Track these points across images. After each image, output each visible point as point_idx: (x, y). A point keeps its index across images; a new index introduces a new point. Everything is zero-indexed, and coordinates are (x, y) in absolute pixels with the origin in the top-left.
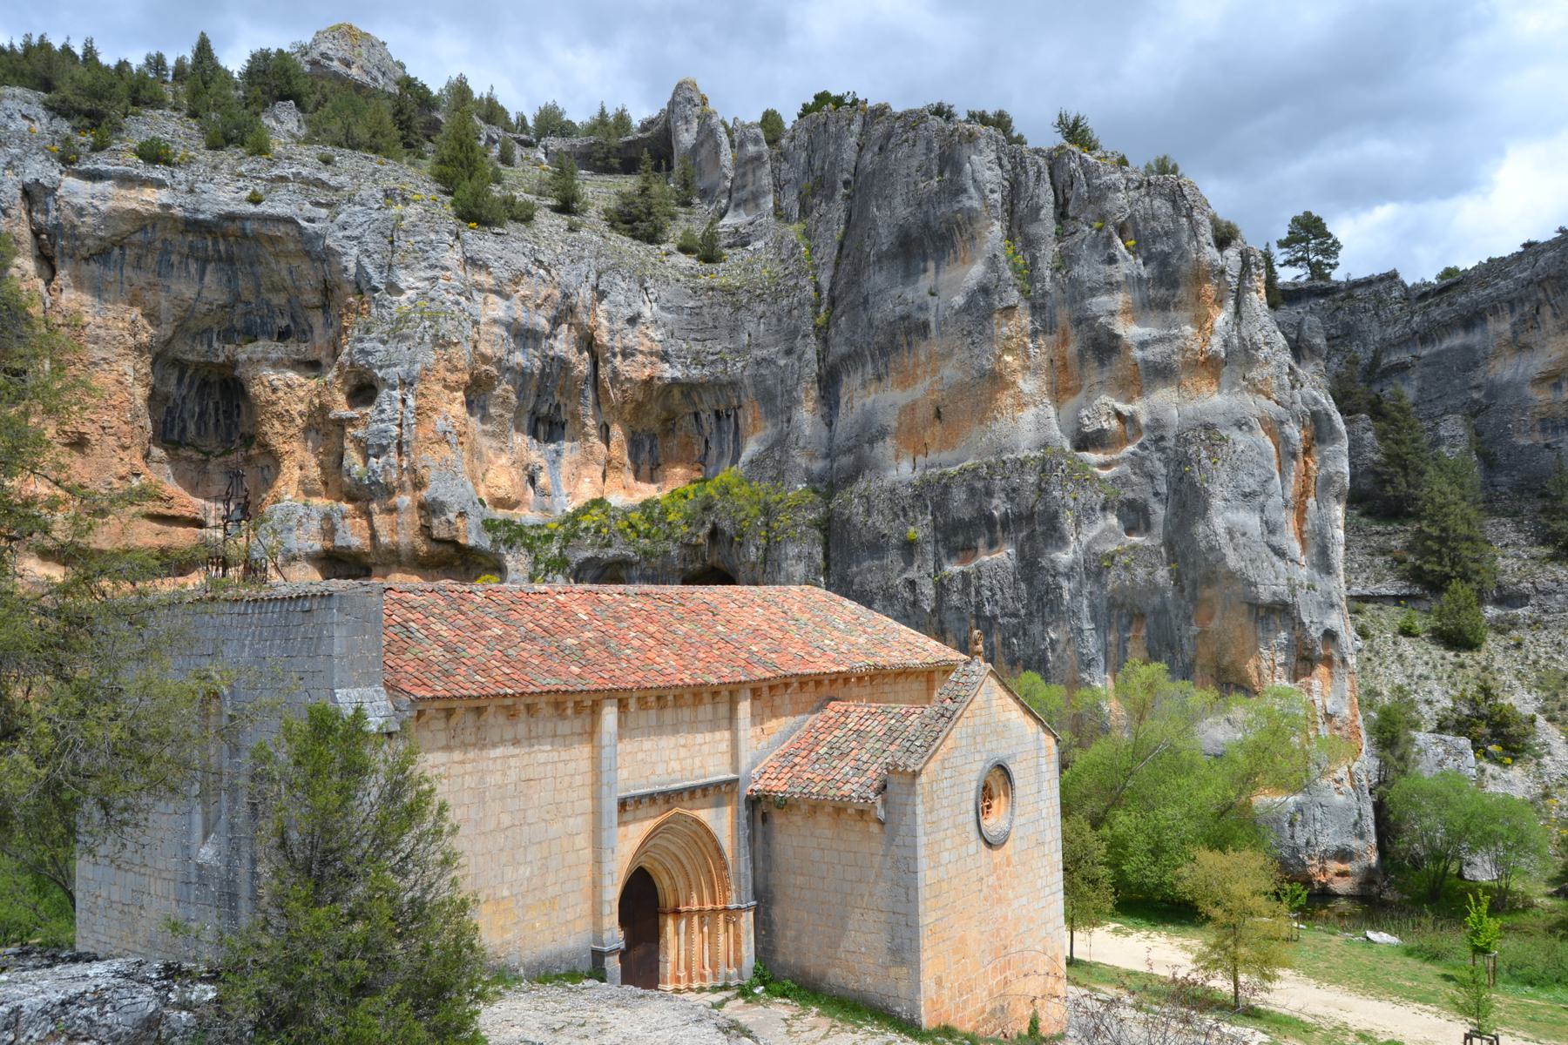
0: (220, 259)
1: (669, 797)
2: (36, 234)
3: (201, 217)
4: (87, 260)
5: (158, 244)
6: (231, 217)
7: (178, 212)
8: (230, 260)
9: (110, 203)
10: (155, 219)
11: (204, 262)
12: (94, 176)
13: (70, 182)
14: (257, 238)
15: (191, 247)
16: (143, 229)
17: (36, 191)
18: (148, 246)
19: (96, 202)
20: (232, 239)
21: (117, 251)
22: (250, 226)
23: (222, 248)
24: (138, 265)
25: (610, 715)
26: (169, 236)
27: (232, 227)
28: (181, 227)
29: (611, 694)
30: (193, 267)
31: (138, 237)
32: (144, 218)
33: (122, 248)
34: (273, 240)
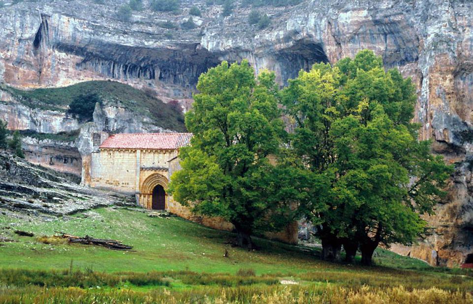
0: (389, 33)
1: (152, 169)
2: (334, 37)
3: (377, 18)
4: (349, 42)
5: (368, 32)
6: (386, 17)
7: (370, 18)
8: (392, 33)
9: (351, 20)
10: (363, 22)
11: (385, 35)
12: (347, 11)
13: (342, 15)
14: (393, 23)
15: (379, 30)
16: (361, 27)
17: (331, 21)
18: (364, 33)
19: (347, 20)
20: (389, 24)
21: (356, 37)
22: (392, 18)
23: (388, 29)
24: (364, 42)
25: (138, 151)
26: (370, 28)
27: (386, 20)
28: (373, 23)
29: (139, 149)
30: (382, 37)
31: (361, 30)
32: (361, 23)
33: (358, 36)
34: (399, 22)
